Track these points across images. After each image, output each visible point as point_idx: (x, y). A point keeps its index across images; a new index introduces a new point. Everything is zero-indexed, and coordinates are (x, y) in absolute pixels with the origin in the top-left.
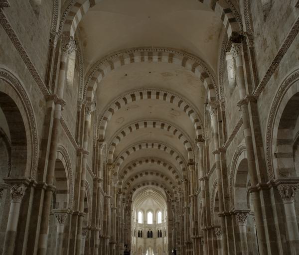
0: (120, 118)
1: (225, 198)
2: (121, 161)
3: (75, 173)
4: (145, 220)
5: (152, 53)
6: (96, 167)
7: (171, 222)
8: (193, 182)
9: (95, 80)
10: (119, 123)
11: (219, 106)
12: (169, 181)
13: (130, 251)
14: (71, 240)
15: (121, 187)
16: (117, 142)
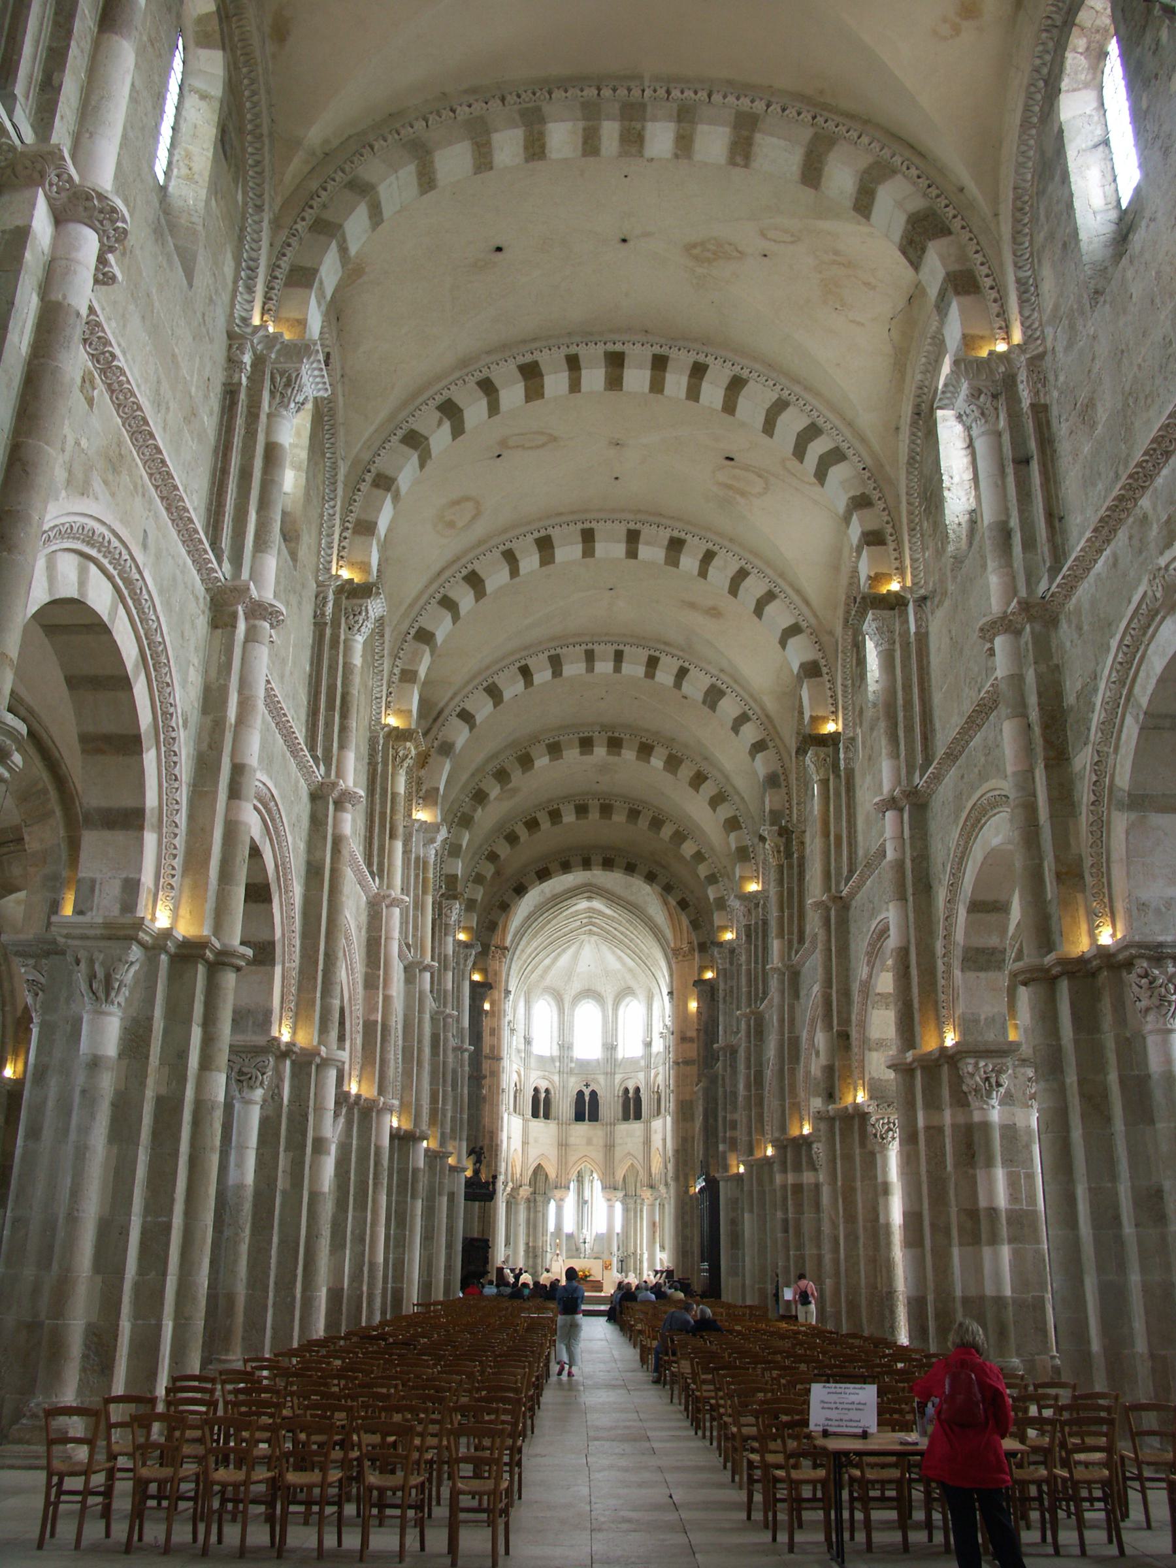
0: (457, 502)
1: (1059, 876)
2: (460, 736)
3: (194, 717)
4: (565, 1047)
5: (643, 106)
6: (329, 725)
7: (687, 1045)
8: (826, 834)
9: (333, 236)
10: (451, 525)
11: (1010, 382)
13: (495, 1177)
14: (160, 1101)
15: (459, 868)
16: (443, 628)
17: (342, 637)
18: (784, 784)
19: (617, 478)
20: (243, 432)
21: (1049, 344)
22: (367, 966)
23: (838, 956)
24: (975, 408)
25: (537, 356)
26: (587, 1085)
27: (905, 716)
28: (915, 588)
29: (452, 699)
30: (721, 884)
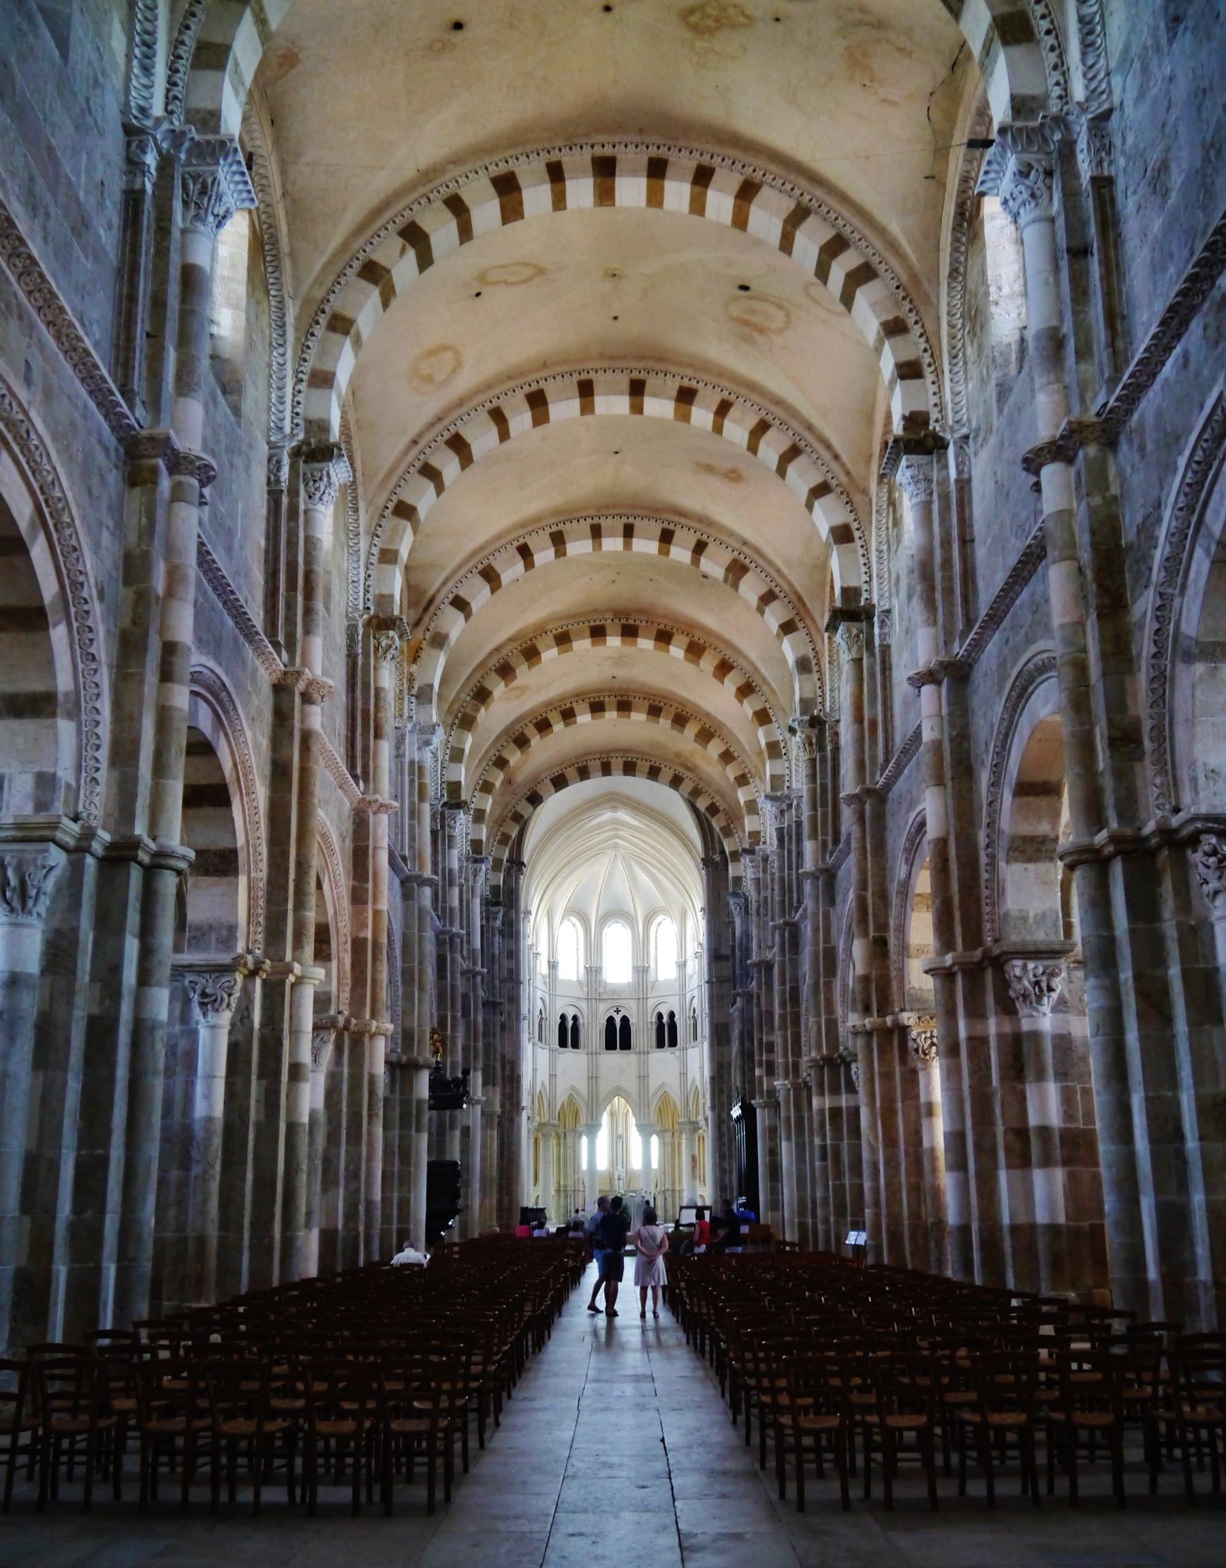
1: (1112, 743)
2: (454, 625)
4: (593, 971)
6: (290, 606)
7: (726, 965)
8: (858, 718)
10: (429, 379)
12: (715, 748)
16: (424, 498)
17: (302, 507)
18: (815, 668)
19: (615, 318)
20: (152, 250)
21: (1116, 99)
22: (354, 879)
23: (874, 854)
24: (1023, 190)
25: (513, 166)
26: (618, 1011)
27: (943, 577)
28: (956, 427)
29: (444, 583)
30: (751, 786)
